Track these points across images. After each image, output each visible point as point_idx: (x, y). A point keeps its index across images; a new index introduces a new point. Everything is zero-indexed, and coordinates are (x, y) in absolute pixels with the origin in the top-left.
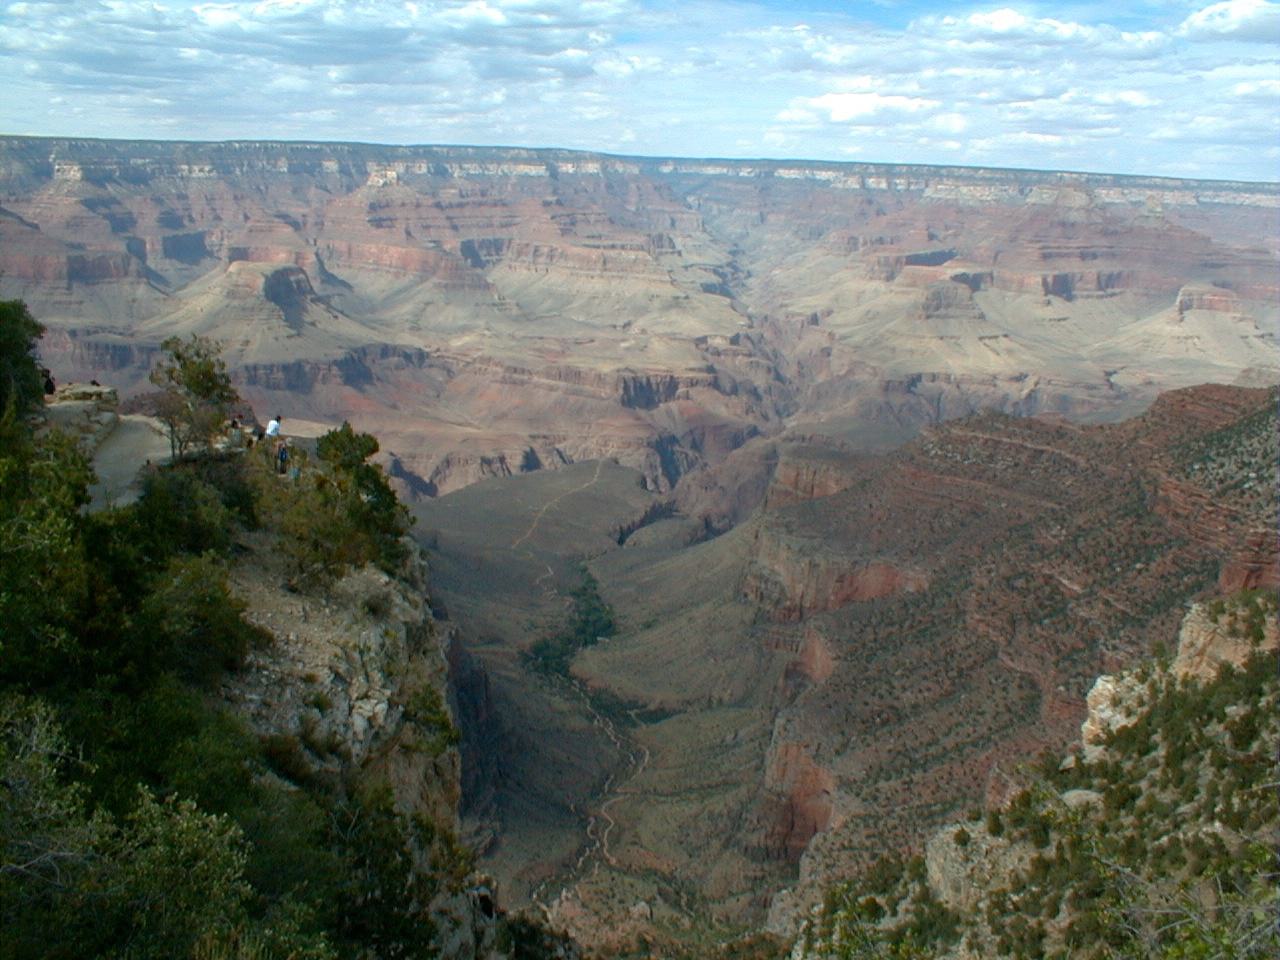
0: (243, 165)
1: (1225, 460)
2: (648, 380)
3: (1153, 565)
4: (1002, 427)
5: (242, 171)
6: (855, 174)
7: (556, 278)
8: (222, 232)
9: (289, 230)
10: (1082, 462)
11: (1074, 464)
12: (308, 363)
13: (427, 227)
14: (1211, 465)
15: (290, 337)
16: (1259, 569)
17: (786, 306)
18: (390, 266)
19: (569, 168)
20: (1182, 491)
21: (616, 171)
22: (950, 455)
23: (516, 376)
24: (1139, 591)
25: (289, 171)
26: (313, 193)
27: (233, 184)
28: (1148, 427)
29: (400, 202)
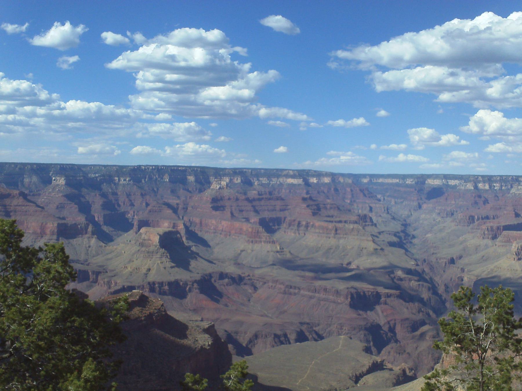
2: (364, 292)
5: (145, 180)
6: (470, 181)
7: (311, 239)
8: (134, 212)
9: (169, 212)
12: (181, 281)
13: (241, 211)
15: (172, 267)
18: (222, 230)
19: (314, 180)
21: (340, 182)
25: (170, 181)
26: (181, 192)
27: (141, 188)
29: (227, 197)
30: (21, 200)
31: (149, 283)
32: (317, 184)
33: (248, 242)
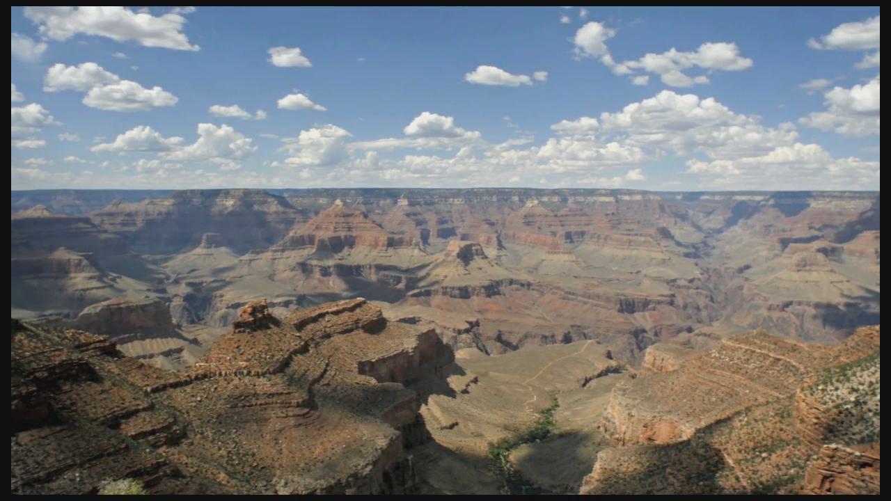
0: (477, 198)
1: (840, 385)
2: (633, 302)
3: (774, 456)
4: (758, 342)
7: (607, 251)
9: (487, 226)
10: (802, 369)
11: (798, 370)
13: (550, 226)
14: (830, 387)
15: (465, 274)
16: (831, 476)
17: (726, 264)
18: (531, 242)
19: (627, 198)
20: (807, 404)
22: (723, 357)
23: (570, 296)
24: (759, 473)
26: (506, 210)
27: (473, 207)
28: (848, 350)
30: (361, 219)
31: (443, 288)
32: (629, 201)
33: (549, 253)
